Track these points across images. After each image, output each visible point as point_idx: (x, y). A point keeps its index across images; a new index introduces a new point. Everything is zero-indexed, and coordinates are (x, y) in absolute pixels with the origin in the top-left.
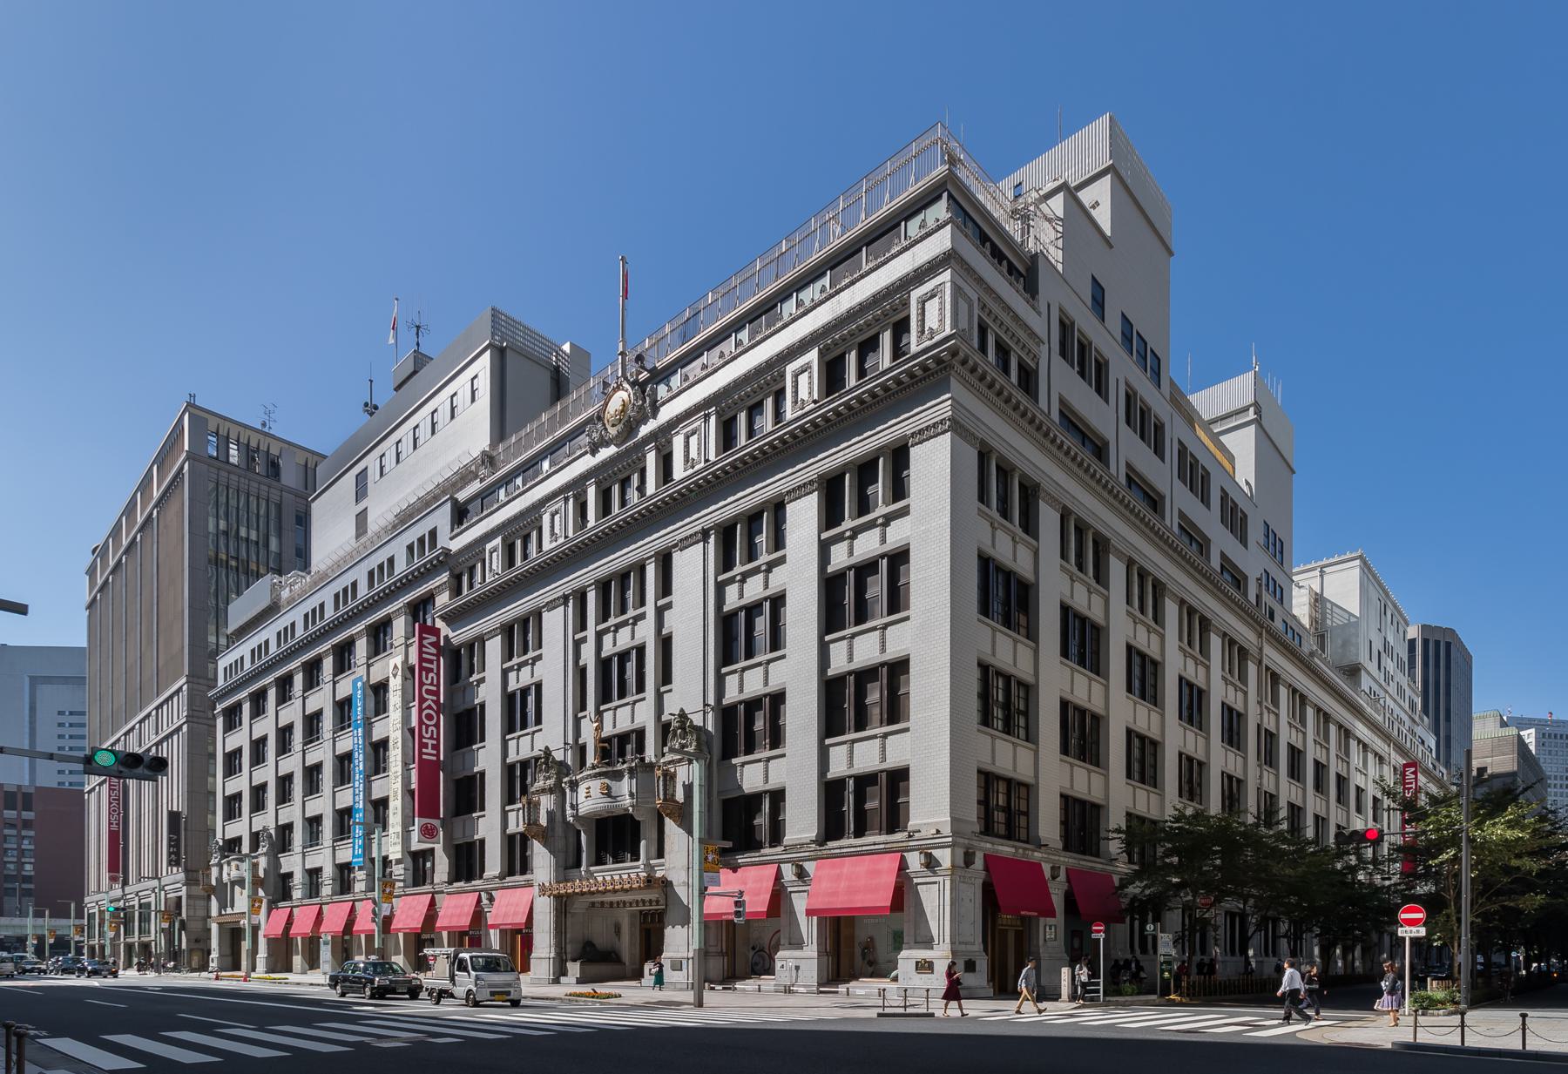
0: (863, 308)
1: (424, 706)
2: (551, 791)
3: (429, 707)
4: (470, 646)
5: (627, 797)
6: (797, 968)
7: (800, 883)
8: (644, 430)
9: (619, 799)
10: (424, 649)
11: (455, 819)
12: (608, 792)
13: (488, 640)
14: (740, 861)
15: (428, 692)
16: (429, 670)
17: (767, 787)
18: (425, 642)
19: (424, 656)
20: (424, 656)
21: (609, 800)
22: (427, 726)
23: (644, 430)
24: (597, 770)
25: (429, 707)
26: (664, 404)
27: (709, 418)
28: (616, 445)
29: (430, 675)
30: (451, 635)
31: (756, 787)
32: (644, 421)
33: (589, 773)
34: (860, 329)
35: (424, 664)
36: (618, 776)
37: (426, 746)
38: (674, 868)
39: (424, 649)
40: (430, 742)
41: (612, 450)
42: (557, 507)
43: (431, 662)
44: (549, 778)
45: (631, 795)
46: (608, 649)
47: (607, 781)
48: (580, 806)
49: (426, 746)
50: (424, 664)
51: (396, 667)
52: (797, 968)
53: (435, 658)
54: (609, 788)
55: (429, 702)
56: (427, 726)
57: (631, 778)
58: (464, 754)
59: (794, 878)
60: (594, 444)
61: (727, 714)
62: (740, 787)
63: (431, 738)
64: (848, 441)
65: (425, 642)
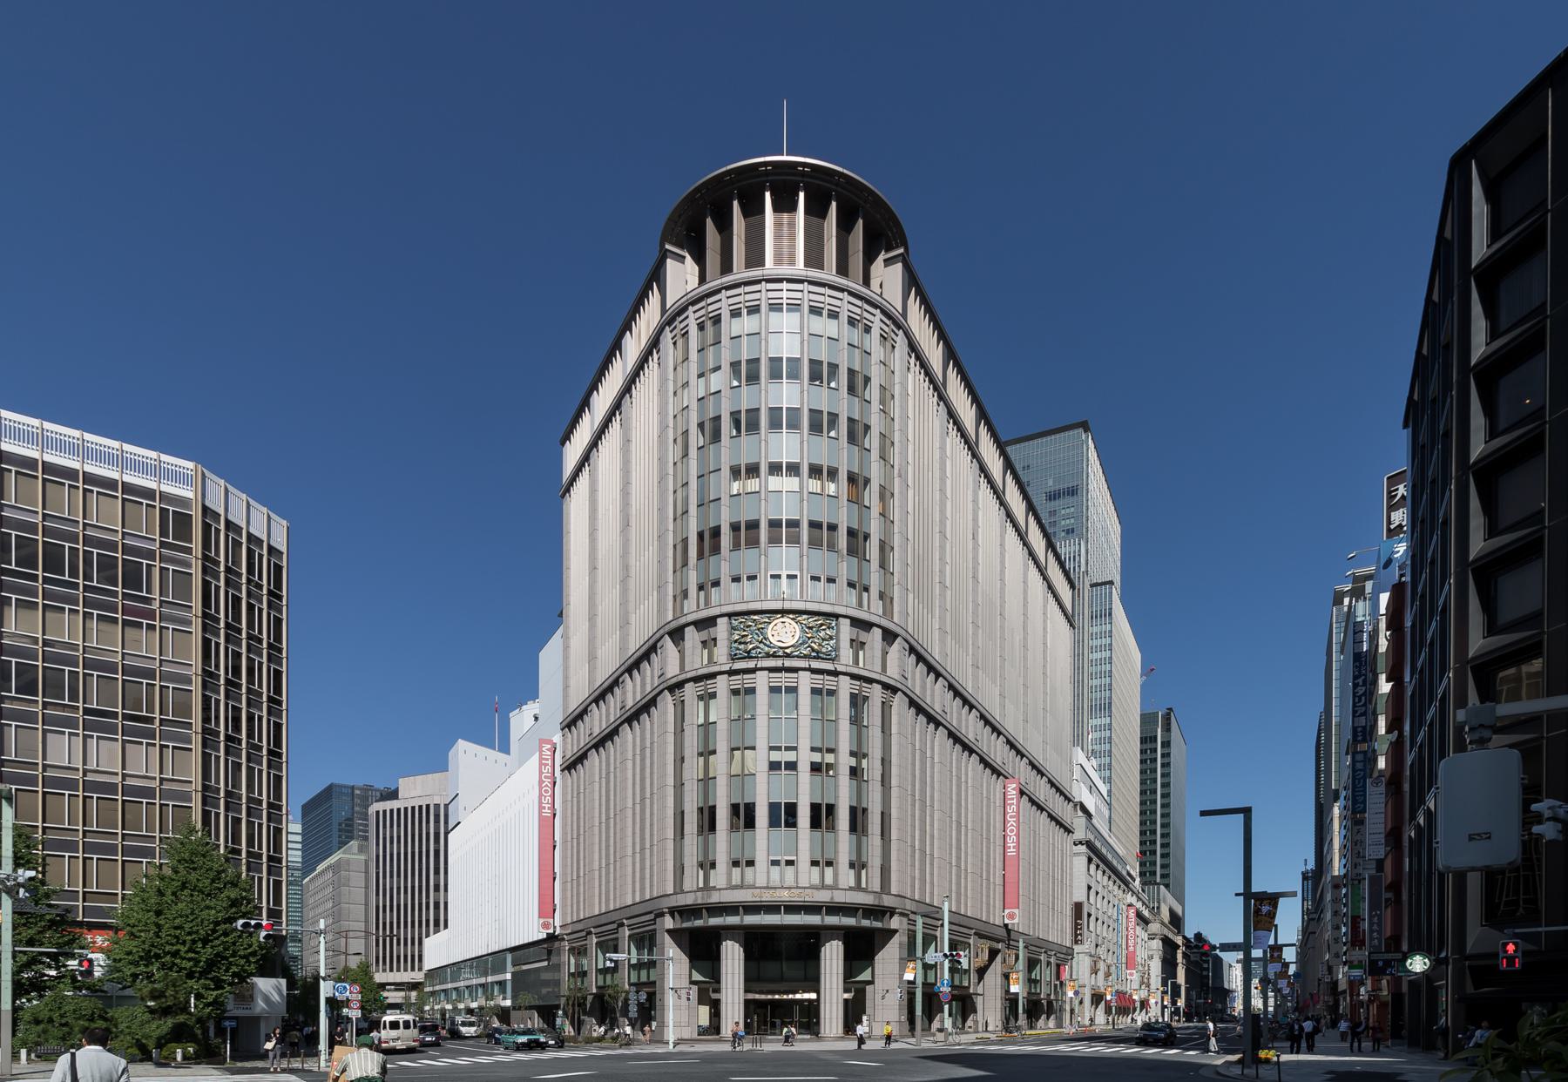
22: (545, 797)
37: (544, 808)
40: (547, 806)
49: (544, 808)
56: (545, 797)
63: (548, 803)
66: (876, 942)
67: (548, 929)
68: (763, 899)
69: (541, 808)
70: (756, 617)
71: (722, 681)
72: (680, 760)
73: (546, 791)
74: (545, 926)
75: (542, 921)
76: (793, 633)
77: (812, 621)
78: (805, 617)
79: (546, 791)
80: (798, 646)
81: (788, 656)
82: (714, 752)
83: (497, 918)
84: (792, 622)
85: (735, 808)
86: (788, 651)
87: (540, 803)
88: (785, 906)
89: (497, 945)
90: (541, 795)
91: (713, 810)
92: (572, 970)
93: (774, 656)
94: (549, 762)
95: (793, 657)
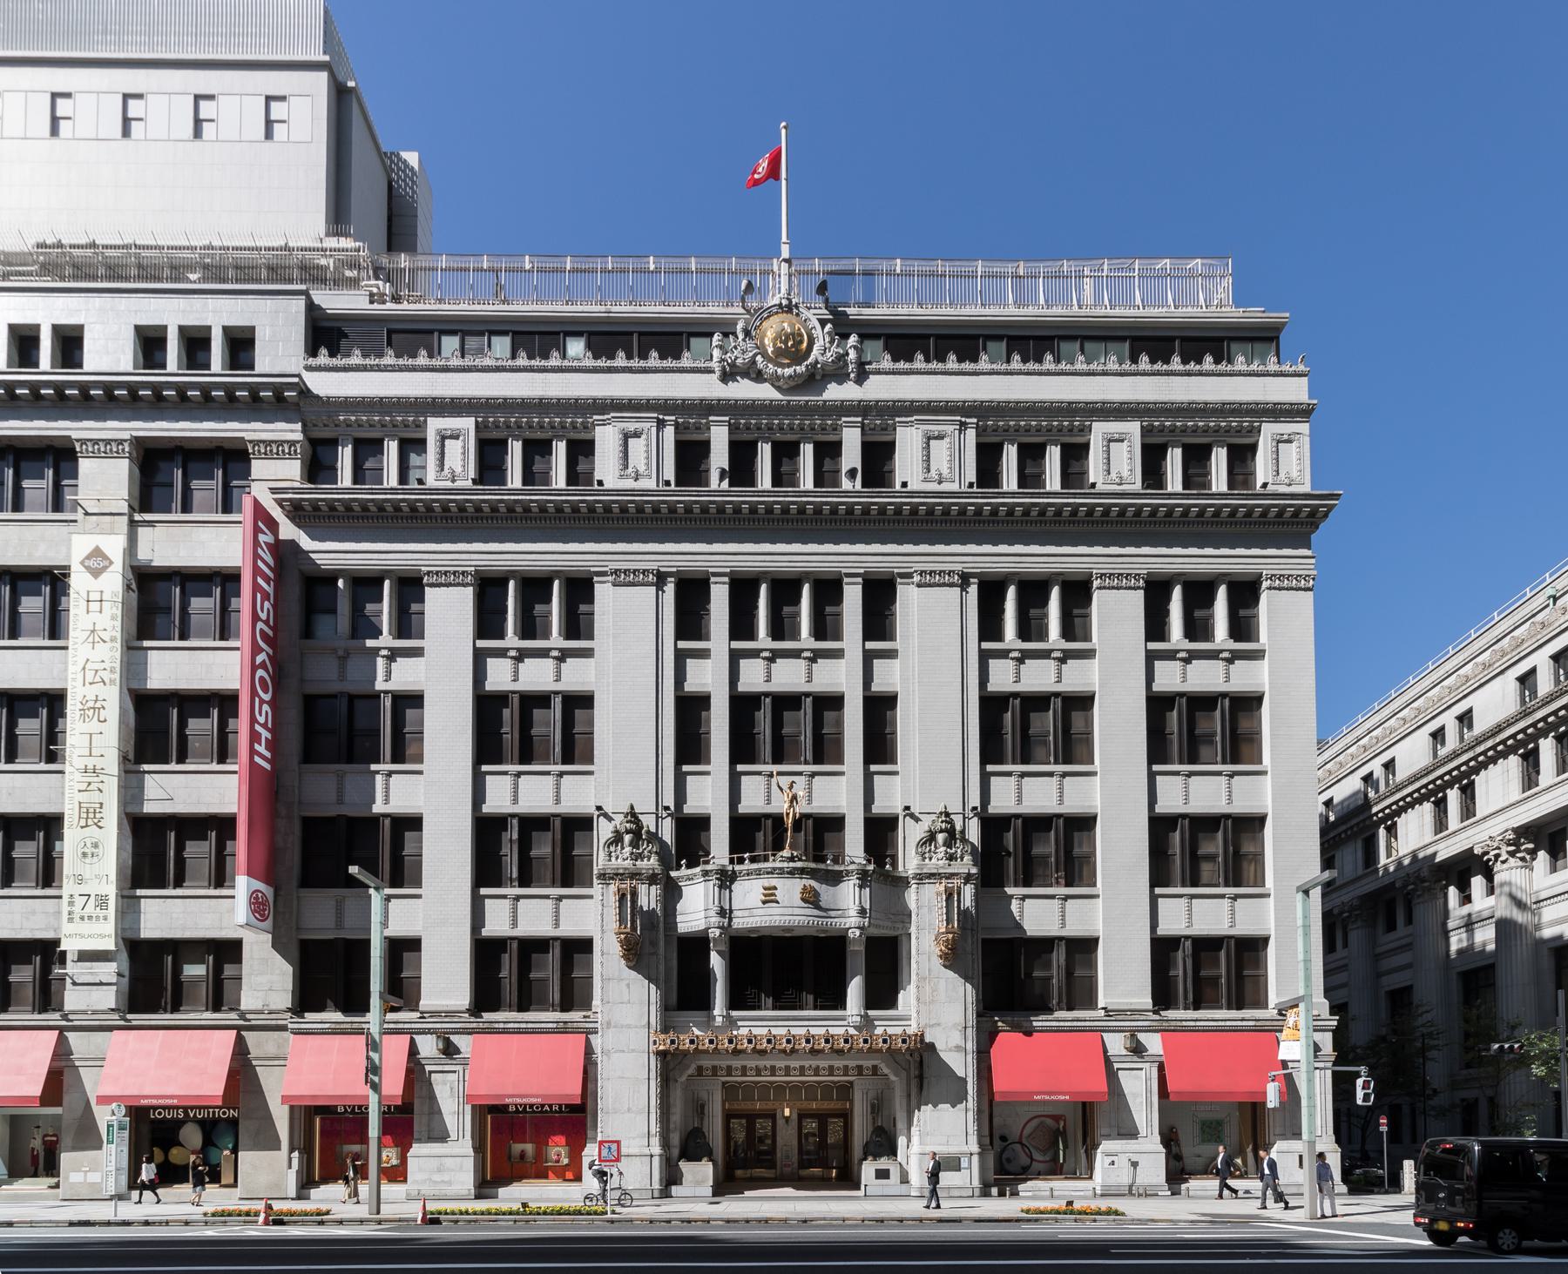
0: (1204, 410)
2: (652, 879)
4: (366, 584)
5: (853, 912)
6: (1135, 1164)
7: (1135, 1059)
8: (835, 392)
9: (832, 913)
11: (305, 892)
12: (811, 898)
13: (432, 585)
14: (1035, 1024)
17: (1064, 933)
21: (816, 912)
23: (835, 392)
24: (799, 864)
26: (878, 372)
27: (966, 429)
28: (778, 388)
30: (306, 543)
31: (1049, 931)
32: (840, 376)
33: (778, 865)
34: (1195, 430)
36: (835, 879)
38: (939, 1025)
41: (765, 392)
42: (638, 425)
44: (640, 857)
45: (862, 912)
46: (753, 677)
47: (813, 883)
48: (736, 913)
51: (97, 553)
52: (1135, 1164)
54: (816, 894)
57: (861, 887)
58: (341, 777)
59: (1125, 1052)
60: (733, 365)
61: (994, 825)
62: (1019, 926)
64: (1262, 548)
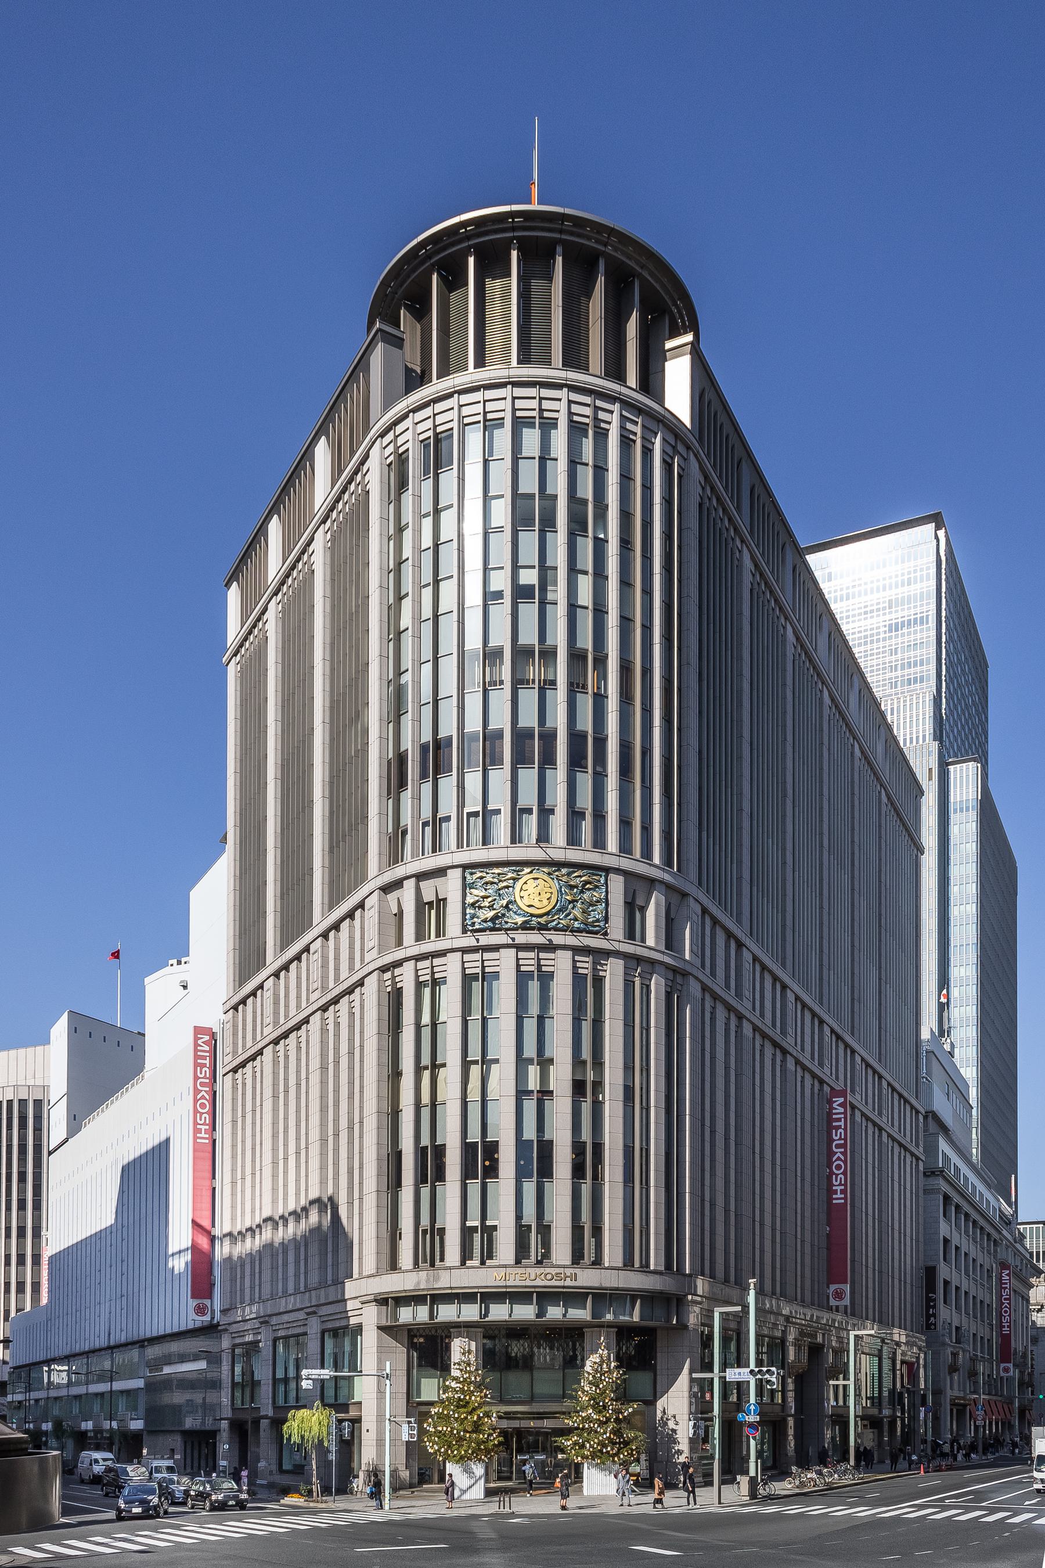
1: (198, 1097)
3: (203, 1097)
10: (199, 1048)
15: (202, 1085)
16: (204, 1065)
18: (200, 1042)
19: (199, 1053)
20: (199, 1053)
25: (203, 1097)
29: (204, 1069)
35: (199, 1061)
39: (199, 1048)
43: (204, 1058)
50: (199, 1061)
53: (208, 1054)
55: (203, 1093)
65: (200, 1042)
66: (659, 1344)
67: (204, 1314)
68: (509, 1284)
69: (197, 1131)
70: (497, 871)
71: (453, 961)
72: (396, 1075)
73: (203, 1106)
74: (200, 1310)
75: (196, 1302)
76: (549, 895)
77: (579, 878)
78: (564, 871)
79: (203, 1106)
80: (555, 914)
81: (542, 928)
82: (444, 1065)
83: (124, 1292)
84: (546, 877)
85: (468, 1150)
86: (542, 920)
87: (195, 1123)
88: (537, 1293)
89: (124, 1334)
90: (196, 1111)
91: (440, 1151)
92: (238, 1379)
93: (525, 927)
94: (207, 1062)
95: (549, 930)
